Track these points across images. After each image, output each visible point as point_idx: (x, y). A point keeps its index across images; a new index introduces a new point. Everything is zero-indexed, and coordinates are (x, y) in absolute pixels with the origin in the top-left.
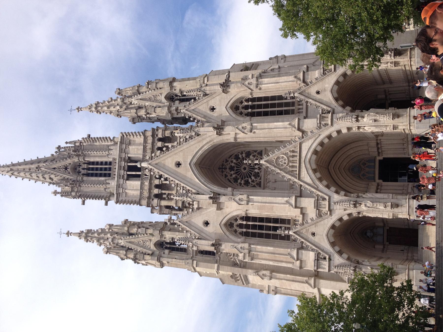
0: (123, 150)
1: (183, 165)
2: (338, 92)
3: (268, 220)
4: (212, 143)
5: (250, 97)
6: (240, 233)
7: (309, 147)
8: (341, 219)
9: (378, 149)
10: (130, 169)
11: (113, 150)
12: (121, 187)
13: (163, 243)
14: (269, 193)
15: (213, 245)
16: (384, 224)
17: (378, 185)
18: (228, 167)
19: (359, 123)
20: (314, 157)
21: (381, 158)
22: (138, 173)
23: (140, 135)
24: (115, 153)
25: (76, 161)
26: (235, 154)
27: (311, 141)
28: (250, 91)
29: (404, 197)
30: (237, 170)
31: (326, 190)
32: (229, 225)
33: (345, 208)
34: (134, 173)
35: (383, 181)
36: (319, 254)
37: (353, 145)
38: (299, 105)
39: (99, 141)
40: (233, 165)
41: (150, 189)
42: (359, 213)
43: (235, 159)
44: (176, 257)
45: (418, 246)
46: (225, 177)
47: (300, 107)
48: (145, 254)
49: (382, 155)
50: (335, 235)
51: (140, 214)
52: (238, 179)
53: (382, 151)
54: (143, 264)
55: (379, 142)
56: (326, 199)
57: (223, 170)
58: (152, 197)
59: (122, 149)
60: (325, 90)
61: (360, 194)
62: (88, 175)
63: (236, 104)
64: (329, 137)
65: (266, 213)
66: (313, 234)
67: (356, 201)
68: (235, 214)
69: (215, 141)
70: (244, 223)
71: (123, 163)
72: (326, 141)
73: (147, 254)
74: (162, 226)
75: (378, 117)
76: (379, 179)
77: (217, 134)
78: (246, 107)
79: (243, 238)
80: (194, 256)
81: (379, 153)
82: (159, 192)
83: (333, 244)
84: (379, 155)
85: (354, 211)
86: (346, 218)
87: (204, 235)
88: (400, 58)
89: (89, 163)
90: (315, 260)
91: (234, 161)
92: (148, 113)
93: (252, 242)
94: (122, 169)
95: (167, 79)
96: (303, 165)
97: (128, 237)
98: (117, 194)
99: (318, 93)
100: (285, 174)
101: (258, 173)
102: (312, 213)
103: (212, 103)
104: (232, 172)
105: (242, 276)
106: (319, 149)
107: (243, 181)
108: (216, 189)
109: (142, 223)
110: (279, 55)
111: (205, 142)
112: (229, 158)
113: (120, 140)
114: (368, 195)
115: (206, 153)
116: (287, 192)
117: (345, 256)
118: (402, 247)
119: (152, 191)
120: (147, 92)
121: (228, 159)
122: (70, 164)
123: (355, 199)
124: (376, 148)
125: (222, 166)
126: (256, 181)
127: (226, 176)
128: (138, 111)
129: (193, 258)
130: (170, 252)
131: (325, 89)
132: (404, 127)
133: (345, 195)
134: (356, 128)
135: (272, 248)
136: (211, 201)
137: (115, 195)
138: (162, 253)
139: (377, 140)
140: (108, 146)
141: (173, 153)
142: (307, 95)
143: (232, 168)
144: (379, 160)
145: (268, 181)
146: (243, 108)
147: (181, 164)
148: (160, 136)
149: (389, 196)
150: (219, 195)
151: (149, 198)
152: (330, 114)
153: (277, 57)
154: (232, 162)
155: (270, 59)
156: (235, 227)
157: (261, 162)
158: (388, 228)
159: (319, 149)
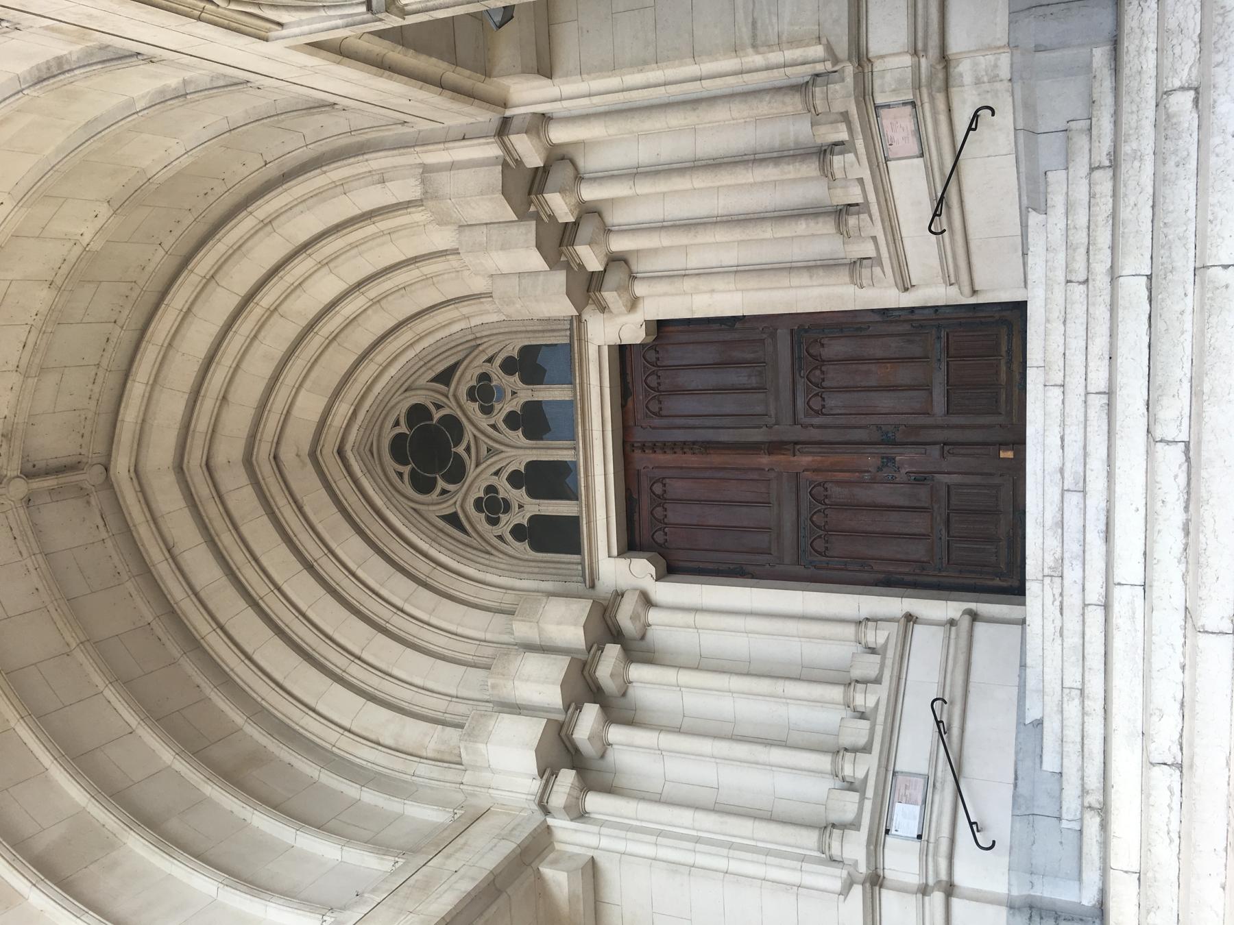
9: (558, 242)
17: (606, 627)
21: (630, 329)
35: (670, 570)
37: (301, 214)
49: (634, 303)
76: (631, 545)
81: (587, 288)
144: (622, 354)
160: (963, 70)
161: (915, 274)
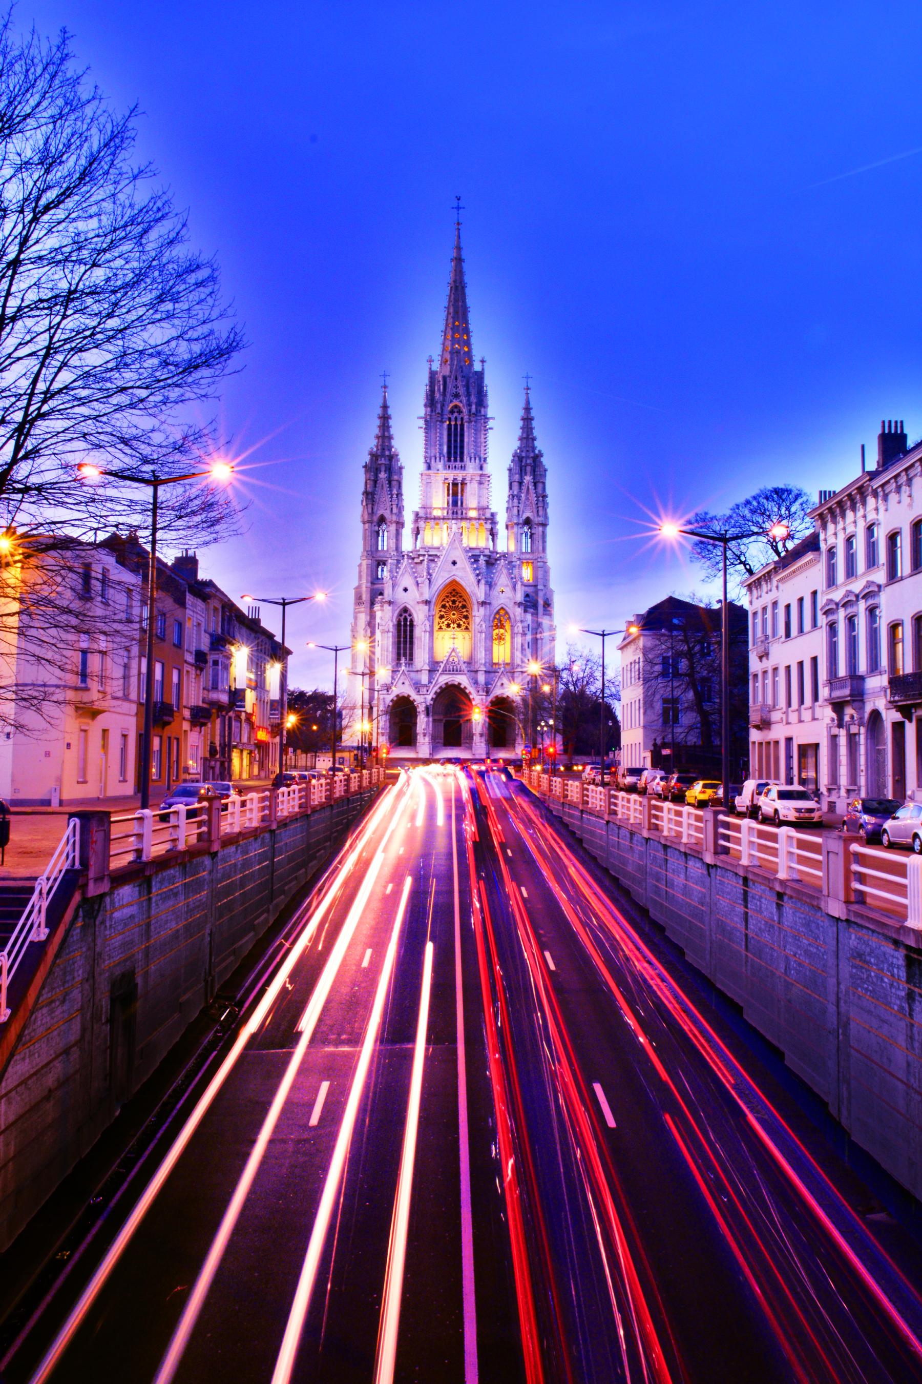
31: (434, 691)
68: (415, 615)
83: (397, 696)
89: (462, 426)
143: (454, 602)
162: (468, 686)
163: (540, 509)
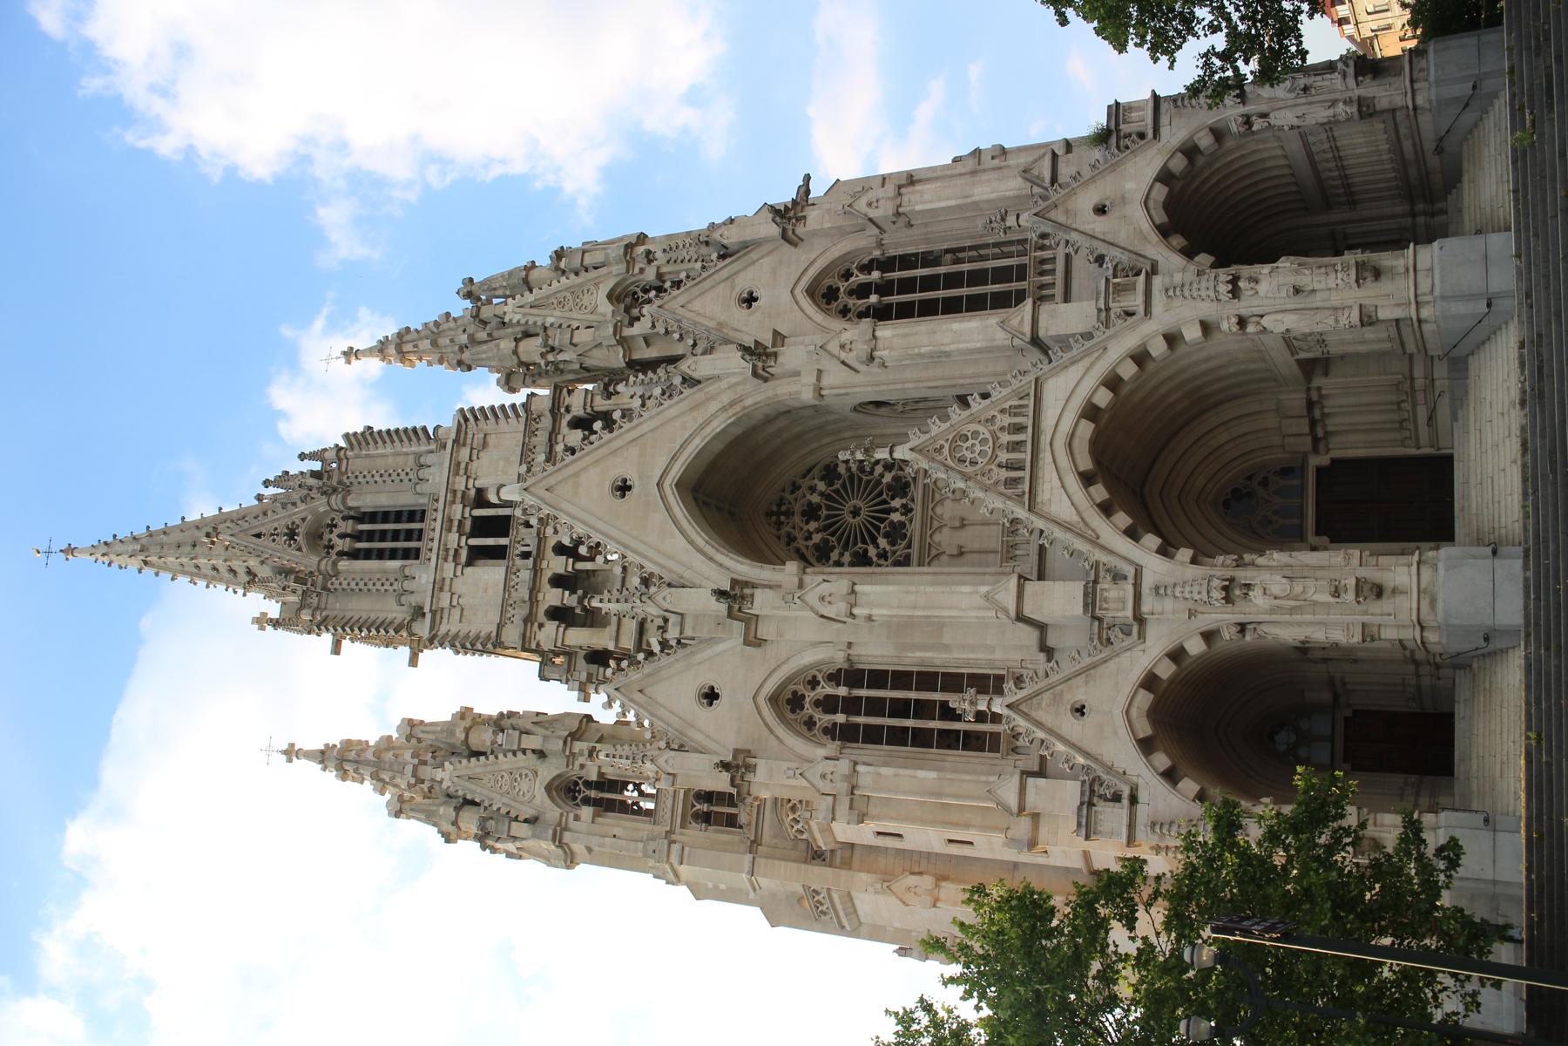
0: (463, 466)
1: (635, 491)
2: (1168, 206)
3: (927, 679)
4: (737, 408)
5: (877, 253)
6: (826, 731)
7: (1068, 392)
8: (1177, 655)
9: (1313, 423)
10: (483, 527)
11: (431, 470)
12: (447, 588)
13: (576, 784)
14: (929, 577)
15: (725, 766)
16: (1336, 697)
18: (798, 508)
19: (1242, 304)
20: (1087, 429)
21: (1324, 460)
22: (503, 541)
23: (518, 416)
24: (437, 477)
25: (322, 509)
26: (827, 461)
27: (1074, 373)
28: (877, 231)
29: (1403, 559)
30: (828, 517)
31: (1124, 545)
32: (788, 702)
33: (1190, 604)
34: (490, 541)
36: (1096, 780)
38: (1042, 274)
39: (393, 442)
40: (815, 499)
41: (534, 590)
42: (1242, 628)
43: (822, 479)
44: (617, 831)
45: (1451, 773)
46: (788, 544)
47: (1047, 279)
48: (516, 819)
49: (1328, 450)
50: (1154, 714)
51: (511, 685)
52: (817, 519)
53: (1327, 434)
54: (510, 855)
55: (1314, 396)
56: (1125, 578)
57: (783, 518)
58: (541, 617)
59: (459, 464)
60: (1124, 200)
61: (1247, 557)
62: (354, 555)
63: (828, 282)
64: (1140, 357)
65: (918, 654)
66: (1080, 711)
67: (1232, 580)
68: (809, 658)
69: (749, 402)
70: (842, 691)
71: (457, 511)
72: (1128, 371)
73: (521, 818)
74: (576, 725)
75: (1306, 279)
76: (1318, 534)
77: (755, 374)
78: (863, 291)
79: (832, 747)
80: (678, 830)
82: (573, 609)
83: (1146, 746)
84: (1316, 450)
85: (1222, 618)
86: (1195, 647)
87: (698, 737)
88: (1375, 83)
89: (362, 517)
90: (1082, 804)
91: (821, 486)
92: (553, 349)
93: (860, 759)
94: (455, 529)
95: (620, 239)
96: (1046, 457)
97: (464, 761)
98: (433, 613)
99: (1101, 210)
100: (981, 495)
101: (902, 525)
102: (1072, 638)
103: (744, 283)
104: (813, 525)
105: (835, 896)
106: (1103, 398)
107: (847, 554)
108: (745, 569)
109: (511, 714)
110: (985, 145)
111: (713, 407)
112: (804, 476)
113: (453, 436)
114: (1276, 555)
115: (718, 447)
116: (992, 570)
117: (1190, 786)
118: (1399, 779)
119: (540, 596)
120: (555, 283)
121: (800, 482)
122: (303, 520)
123: (1228, 573)
124: (1306, 421)
125: (779, 505)
126: (894, 553)
127: (791, 539)
128: (522, 344)
129: (674, 837)
130: (596, 815)
131: (1123, 198)
132: (1398, 313)
133: (1194, 561)
134: (1234, 320)
135: (933, 775)
136: (722, 607)
137: (428, 616)
138: (571, 816)
139: (1309, 389)
140: (418, 456)
141: (604, 450)
142: (1062, 219)
143: (811, 512)
144: (1319, 470)
145: (934, 552)
146: (851, 293)
147: (629, 488)
148: (578, 410)
149: (1348, 559)
150: (754, 586)
151: (528, 620)
152: (1142, 277)
153: (977, 153)
154: (813, 489)
155: (956, 160)
156: (809, 709)
157: (897, 455)
158: (1348, 713)
159: (1103, 398)
160: (1437, 383)
161: (1422, 443)
162: (1101, 369)
163: (588, 260)
